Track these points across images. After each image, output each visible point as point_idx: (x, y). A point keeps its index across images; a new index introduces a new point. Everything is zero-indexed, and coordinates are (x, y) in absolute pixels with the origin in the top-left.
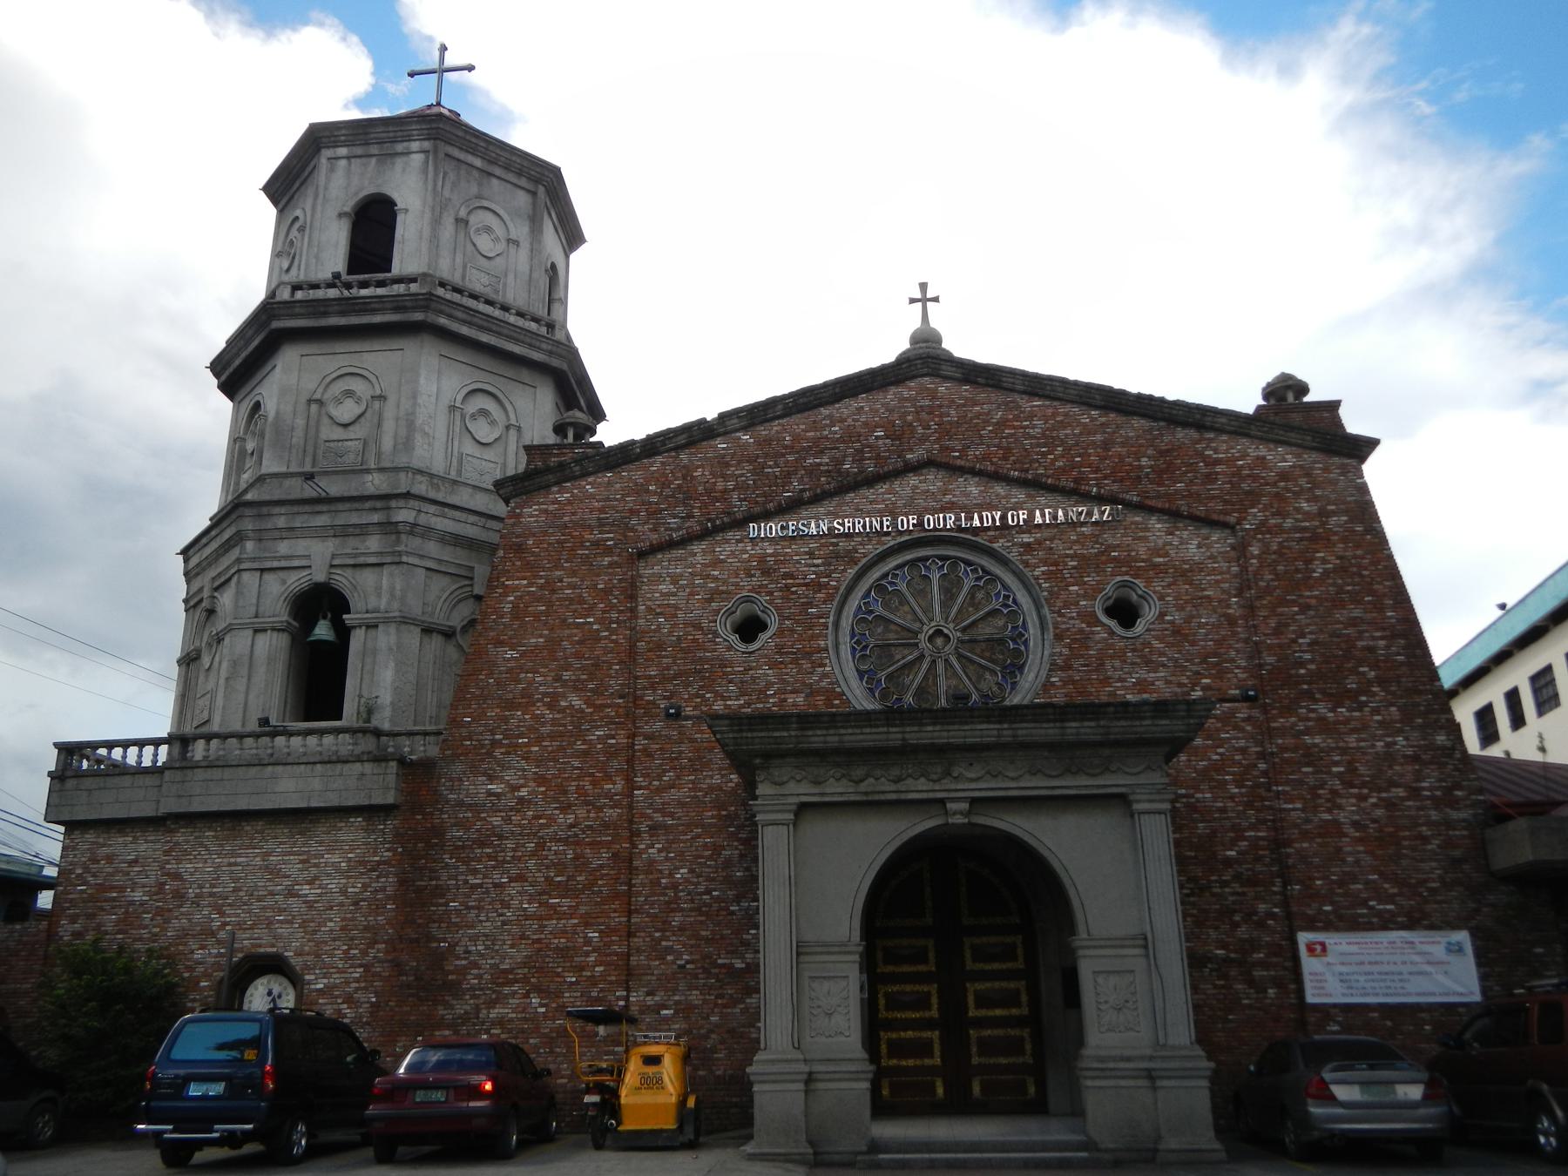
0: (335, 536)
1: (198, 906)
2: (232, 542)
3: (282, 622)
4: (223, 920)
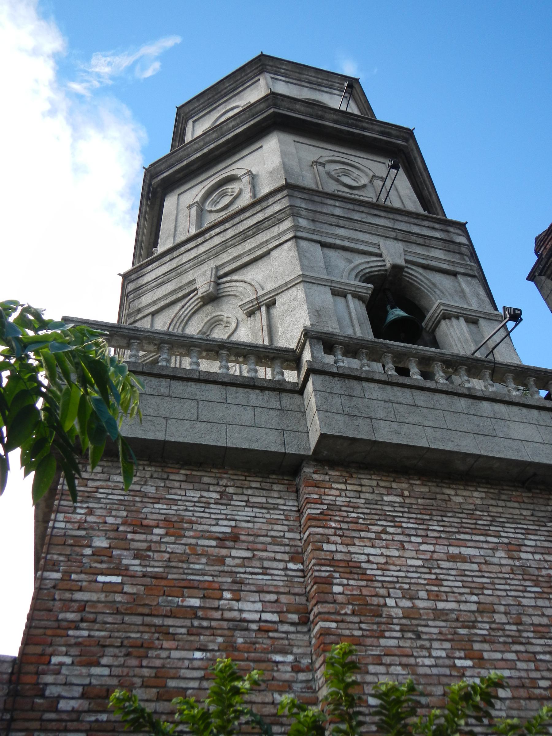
0: (396, 239)
1: (419, 637)
2: (266, 224)
3: (367, 288)
4: (484, 673)
